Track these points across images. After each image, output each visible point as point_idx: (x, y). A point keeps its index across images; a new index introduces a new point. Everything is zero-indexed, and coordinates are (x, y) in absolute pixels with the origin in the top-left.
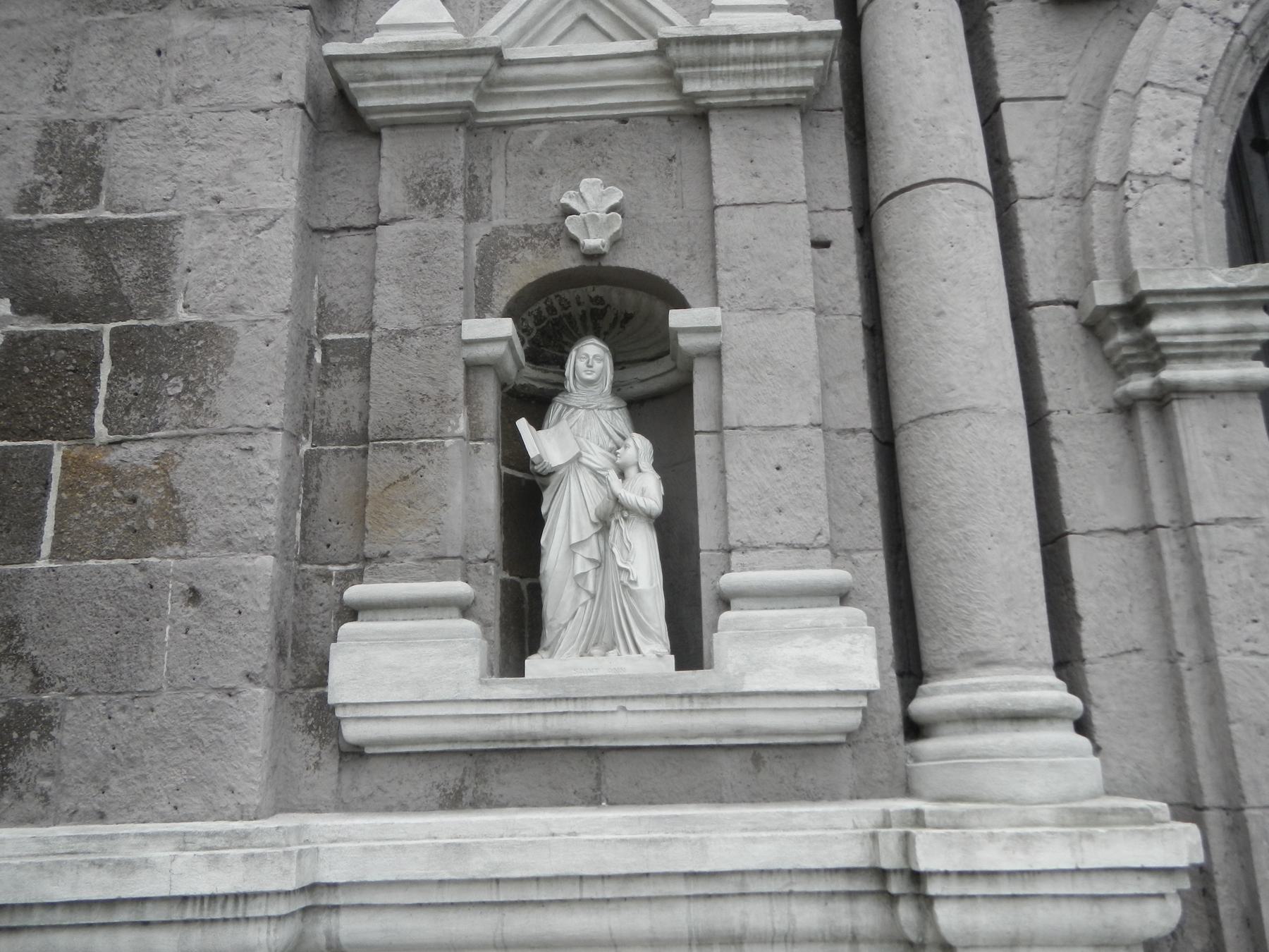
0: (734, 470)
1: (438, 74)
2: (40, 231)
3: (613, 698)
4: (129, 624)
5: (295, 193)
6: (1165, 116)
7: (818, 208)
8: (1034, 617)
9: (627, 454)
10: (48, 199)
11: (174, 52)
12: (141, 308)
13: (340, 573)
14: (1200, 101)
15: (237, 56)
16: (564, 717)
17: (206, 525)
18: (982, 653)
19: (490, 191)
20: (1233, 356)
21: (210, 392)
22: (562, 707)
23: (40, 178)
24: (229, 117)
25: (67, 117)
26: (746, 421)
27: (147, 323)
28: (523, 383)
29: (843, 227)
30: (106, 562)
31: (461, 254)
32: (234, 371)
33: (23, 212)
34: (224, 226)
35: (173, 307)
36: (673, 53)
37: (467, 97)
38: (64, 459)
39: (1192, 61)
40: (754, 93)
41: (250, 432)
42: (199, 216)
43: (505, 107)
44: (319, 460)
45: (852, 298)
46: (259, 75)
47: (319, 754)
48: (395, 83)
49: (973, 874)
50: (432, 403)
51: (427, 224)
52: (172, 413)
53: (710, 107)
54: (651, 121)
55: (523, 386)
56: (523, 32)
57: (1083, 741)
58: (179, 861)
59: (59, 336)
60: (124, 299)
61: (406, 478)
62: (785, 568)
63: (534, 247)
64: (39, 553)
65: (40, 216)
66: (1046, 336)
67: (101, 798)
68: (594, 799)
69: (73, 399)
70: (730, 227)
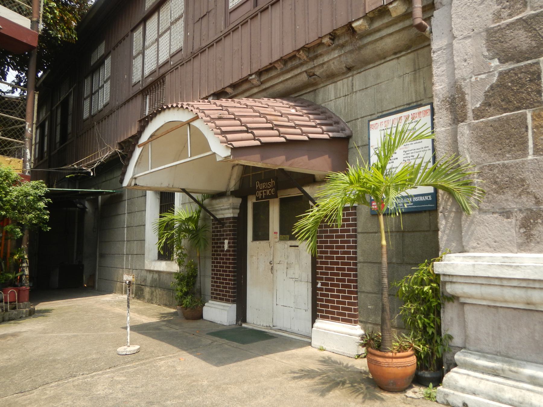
2: (504, 28)
23: (500, 7)
33: (496, 23)
38: (532, 116)
59: (520, 68)
64: (528, 153)
65: (503, 22)
69: (531, 92)
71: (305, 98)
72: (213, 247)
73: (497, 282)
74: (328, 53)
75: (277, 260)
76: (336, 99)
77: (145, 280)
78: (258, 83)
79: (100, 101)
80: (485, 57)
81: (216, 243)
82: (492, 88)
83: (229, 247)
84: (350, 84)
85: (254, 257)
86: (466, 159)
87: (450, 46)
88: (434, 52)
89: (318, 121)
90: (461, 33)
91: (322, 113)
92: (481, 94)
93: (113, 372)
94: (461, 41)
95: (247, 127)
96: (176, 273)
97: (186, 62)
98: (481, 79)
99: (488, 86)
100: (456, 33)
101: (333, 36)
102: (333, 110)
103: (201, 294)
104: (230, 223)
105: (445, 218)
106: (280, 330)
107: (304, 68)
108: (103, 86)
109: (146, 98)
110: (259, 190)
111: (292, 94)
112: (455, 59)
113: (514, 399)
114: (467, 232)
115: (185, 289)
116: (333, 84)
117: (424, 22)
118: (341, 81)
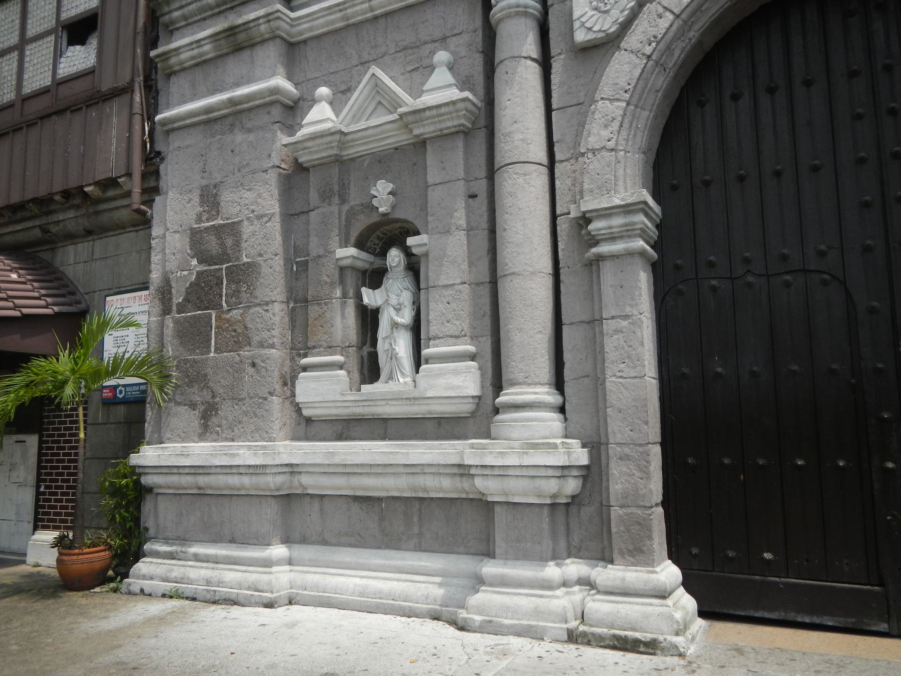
0: (432, 305)
1: (322, 144)
3: (384, 400)
4: (236, 375)
5: (277, 205)
6: (607, 115)
7: (472, 179)
8: (534, 364)
10: (204, 218)
11: (237, 151)
13: (303, 353)
14: (624, 104)
15: (256, 149)
16: (369, 407)
17: (256, 339)
18: (511, 380)
20: (629, 237)
23: (202, 209)
24: (255, 176)
25: (207, 183)
26: (436, 284)
27: (235, 264)
29: (481, 186)
30: (229, 354)
32: (262, 280)
33: (198, 224)
35: (242, 257)
36: (404, 119)
37: (335, 152)
39: (623, 83)
40: (441, 130)
41: (267, 304)
42: (248, 219)
43: (351, 151)
44: (295, 310)
45: (484, 224)
46: (263, 156)
48: (309, 150)
49: (486, 466)
53: (427, 139)
55: (376, 268)
56: (354, 116)
57: (561, 416)
60: (228, 255)
61: (320, 316)
62: (449, 346)
63: (364, 213)
65: (203, 225)
66: (561, 231)
67: (233, 434)
68: (383, 438)
70: (434, 195)
71: (42, 256)
73: (175, 471)
74: (63, 210)
76: (75, 263)
80: (188, 254)
86: (170, 351)
87: (164, 236)
88: (153, 239)
89: (43, 292)
90: (172, 226)
91: (57, 279)
92: (183, 290)
98: (184, 275)
99: (188, 283)
100: (169, 225)
101: (67, 194)
105: (152, 409)
107: (37, 223)
112: (167, 251)
113: (178, 576)
114: (165, 423)
116: (73, 246)
117: (142, 207)
118: (81, 244)
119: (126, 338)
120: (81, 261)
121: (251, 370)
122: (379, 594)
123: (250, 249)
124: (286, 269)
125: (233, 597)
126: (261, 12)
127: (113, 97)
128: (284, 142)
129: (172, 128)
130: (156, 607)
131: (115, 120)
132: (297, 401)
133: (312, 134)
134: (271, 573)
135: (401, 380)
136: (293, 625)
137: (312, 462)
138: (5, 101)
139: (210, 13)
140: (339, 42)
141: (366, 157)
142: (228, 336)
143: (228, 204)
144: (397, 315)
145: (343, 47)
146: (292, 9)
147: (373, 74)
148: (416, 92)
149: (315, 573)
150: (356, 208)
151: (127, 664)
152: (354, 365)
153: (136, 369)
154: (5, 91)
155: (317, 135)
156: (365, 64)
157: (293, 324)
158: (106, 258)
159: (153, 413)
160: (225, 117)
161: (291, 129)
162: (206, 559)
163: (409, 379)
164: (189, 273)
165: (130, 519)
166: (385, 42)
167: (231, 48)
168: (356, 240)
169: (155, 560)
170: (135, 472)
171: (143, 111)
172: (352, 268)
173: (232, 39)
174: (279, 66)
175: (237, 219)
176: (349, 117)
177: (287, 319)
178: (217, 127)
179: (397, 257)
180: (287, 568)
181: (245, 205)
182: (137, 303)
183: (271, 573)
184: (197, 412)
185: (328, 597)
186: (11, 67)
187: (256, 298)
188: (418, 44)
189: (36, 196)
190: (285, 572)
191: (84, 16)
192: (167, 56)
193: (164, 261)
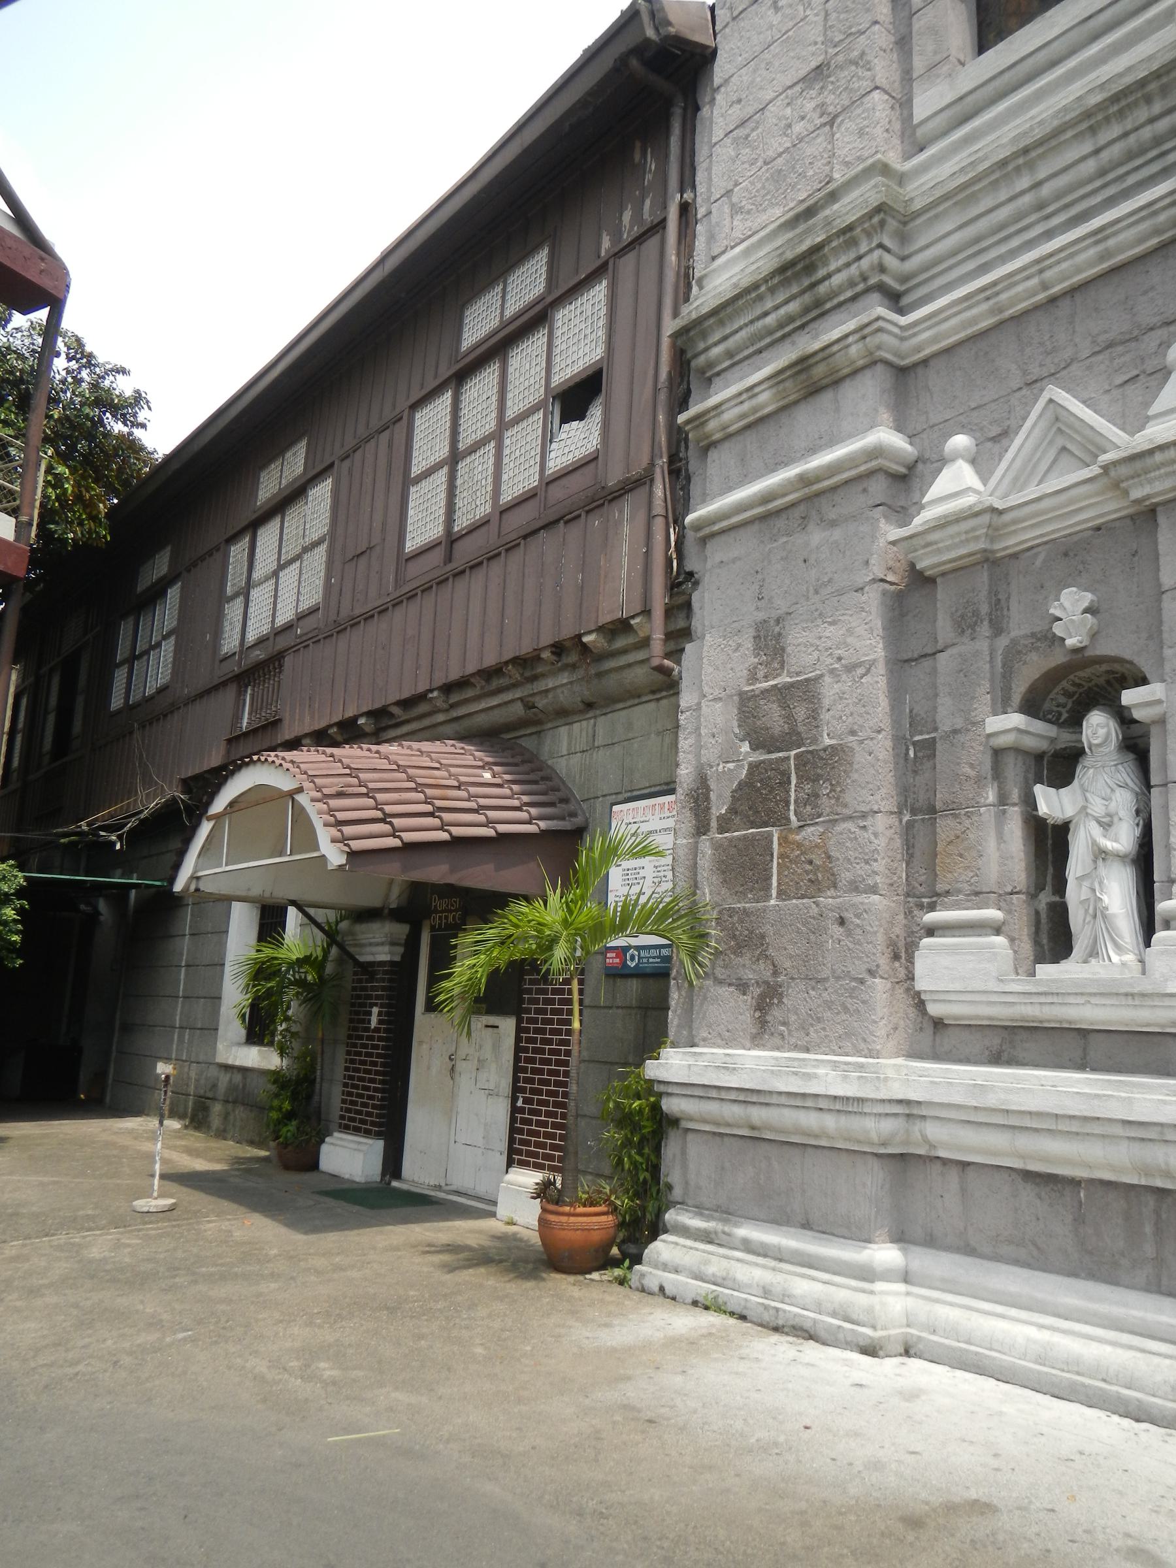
1: (959, 534)
3: (1082, 994)
4: (812, 937)
5: (881, 645)
9: (1113, 806)
10: (760, 674)
11: (812, 561)
12: (807, 739)
13: (928, 903)
15: (844, 552)
16: (1053, 1006)
17: (845, 876)
19: (1008, 609)
21: (842, 791)
22: (1049, 999)
23: (756, 660)
24: (843, 599)
27: (811, 749)
28: (1063, 746)
30: (801, 901)
31: (987, 666)
32: (855, 776)
33: (750, 684)
34: (844, 677)
35: (822, 736)
36: (1113, 473)
37: (981, 545)
41: (864, 816)
42: (832, 671)
43: (1011, 541)
44: (913, 826)
47: (922, 1022)
48: (935, 547)
50: (973, 781)
51: (966, 647)
52: (825, 803)
54: (1117, 524)
55: (1065, 749)
56: (1016, 479)
58: (829, 1076)
59: (770, 761)
60: (799, 734)
63: (1037, 649)
65: (758, 685)
67: (807, 1039)
68: (1081, 1066)
72: (351, 1021)
73: (714, 1094)
74: (554, 673)
75: (462, 1053)
76: (569, 754)
77: (214, 1086)
78: (445, 706)
79: (152, 676)
80: (736, 735)
81: (357, 1013)
82: (740, 784)
83: (380, 1022)
84: (590, 731)
85: (425, 1046)
86: (706, 894)
87: (699, 706)
89: (525, 799)
90: (712, 691)
93: (122, 1233)
94: (711, 703)
95: (384, 813)
96: (274, 1072)
97: (325, 638)
99: (736, 783)
100: (706, 689)
101: (558, 649)
102: (563, 774)
103: (319, 1120)
104: (385, 972)
105: (679, 988)
106: (458, 1193)
107: (518, 693)
108: (159, 645)
109: (246, 692)
110: (436, 911)
111: (501, 733)
112: (703, 731)
113: (718, 1274)
115: (287, 1106)
116: (567, 727)
117: (666, 662)
118: (578, 724)
119: (641, 871)
120: (578, 750)
121: (837, 930)
122: (1074, 1364)
123: (835, 722)
124: (896, 756)
125: (807, 1325)
126: (851, 325)
127: (625, 493)
128: (891, 538)
129: (709, 534)
130: (685, 1322)
131: (626, 529)
132: (917, 988)
133: (939, 518)
134: (872, 1292)
135: (1115, 958)
136: (912, 1395)
137: (945, 1100)
138: (478, 517)
139: (768, 340)
140: (986, 353)
141: (1040, 549)
142: (799, 871)
143: (799, 648)
144: (1105, 836)
145: (993, 361)
146: (902, 312)
147: (1051, 401)
148: (1134, 422)
149: (951, 1304)
150: (1022, 642)
151: (639, 1411)
152: (1022, 925)
153: (655, 922)
154: (478, 503)
155: (949, 519)
156: (1034, 384)
157: (910, 852)
158: (613, 744)
159: (680, 994)
160: (793, 505)
161: (902, 513)
162: (762, 1251)
163: (1130, 958)
164: (735, 766)
165: (644, 1166)
166: (1071, 340)
167: (802, 392)
168: (1023, 698)
169: (682, 1241)
170: (652, 1090)
171: (667, 511)
172: (1017, 750)
173: (803, 376)
174: (882, 410)
175: (813, 674)
176: (1006, 481)
177: (898, 843)
178: (780, 523)
179: (1102, 727)
180: (901, 1287)
181: (827, 650)
182: (657, 817)
183: (872, 1292)
184: (748, 998)
185: (977, 1354)
186: (485, 466)
187: (846, 806)
188: (1136, 333)
189: (517, 654)
190: (897, 1294)
191: (584, 376)
192: (702, 420)
193: (699, 746)
